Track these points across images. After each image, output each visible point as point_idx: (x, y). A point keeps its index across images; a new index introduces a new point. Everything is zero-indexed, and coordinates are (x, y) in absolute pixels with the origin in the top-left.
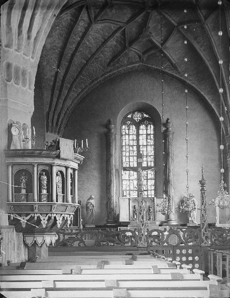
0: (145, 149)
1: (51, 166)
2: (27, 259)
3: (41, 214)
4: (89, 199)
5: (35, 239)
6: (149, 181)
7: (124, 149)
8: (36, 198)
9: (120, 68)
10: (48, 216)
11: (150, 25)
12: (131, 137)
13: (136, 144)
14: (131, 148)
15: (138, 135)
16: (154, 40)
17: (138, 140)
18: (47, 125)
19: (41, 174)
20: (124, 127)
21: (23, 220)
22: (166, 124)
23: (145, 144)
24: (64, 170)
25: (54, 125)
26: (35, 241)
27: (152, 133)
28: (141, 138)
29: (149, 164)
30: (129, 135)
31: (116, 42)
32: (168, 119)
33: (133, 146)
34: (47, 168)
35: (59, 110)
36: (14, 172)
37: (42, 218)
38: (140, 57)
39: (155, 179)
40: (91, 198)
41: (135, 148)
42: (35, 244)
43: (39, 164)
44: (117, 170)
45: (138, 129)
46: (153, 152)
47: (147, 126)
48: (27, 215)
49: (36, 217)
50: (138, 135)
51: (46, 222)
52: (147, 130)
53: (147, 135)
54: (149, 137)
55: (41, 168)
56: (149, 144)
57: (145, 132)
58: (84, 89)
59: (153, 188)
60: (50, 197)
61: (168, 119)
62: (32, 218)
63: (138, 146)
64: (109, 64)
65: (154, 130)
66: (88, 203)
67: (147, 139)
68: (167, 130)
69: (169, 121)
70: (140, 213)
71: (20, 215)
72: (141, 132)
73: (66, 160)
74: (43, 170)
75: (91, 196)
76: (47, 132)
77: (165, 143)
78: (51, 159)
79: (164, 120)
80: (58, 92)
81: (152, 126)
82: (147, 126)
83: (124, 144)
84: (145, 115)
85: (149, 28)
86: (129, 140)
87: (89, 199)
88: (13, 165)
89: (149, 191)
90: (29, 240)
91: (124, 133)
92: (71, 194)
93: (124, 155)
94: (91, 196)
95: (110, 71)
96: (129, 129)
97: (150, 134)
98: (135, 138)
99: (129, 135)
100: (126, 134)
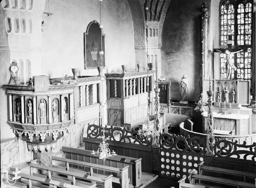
0: (242, 28)
2: (33, 158)
3: (29, 132)
4: (183, 78)
6: (246, 60)
7: (222, 29)
12: (229, 17)
13: (234, 23)
14: (229, 27)
15: (236, 14)
17: (236, 19)
20: (222, 7)
23: (243, 22)
24: (46, 98)
27: (250, 11)
28: (239, 17)
29: (247, 43)
30: (227, 14)
33: (231, 25)
34: (31, 98)
36: (14, 99)
37: (29, 135)
39: (252, 58)
41: (233, 27)
44: (209, 51)
45: (236, 8)
46: (250, 31)
47: (245, 5)
50: (236, 14)
51: (32, 138)
52: (245, 8)
53: (245, 13)
54: (246, 16)
56: (247, 23)
57: (243, 11)
59: (249, 67)
63: (236, 25)
67: (245, 18)
71: (19, 131)
72: (239, 11)
73: (152, 48)
82: (245, 5)
83: (222, 23)
86: (227, 20)
89: (246, 70)
91: (222, 13)
93: (222, 34)
96: (227, 9)
97: (248, 13)
98: (233, 17)
99: (227, 14)
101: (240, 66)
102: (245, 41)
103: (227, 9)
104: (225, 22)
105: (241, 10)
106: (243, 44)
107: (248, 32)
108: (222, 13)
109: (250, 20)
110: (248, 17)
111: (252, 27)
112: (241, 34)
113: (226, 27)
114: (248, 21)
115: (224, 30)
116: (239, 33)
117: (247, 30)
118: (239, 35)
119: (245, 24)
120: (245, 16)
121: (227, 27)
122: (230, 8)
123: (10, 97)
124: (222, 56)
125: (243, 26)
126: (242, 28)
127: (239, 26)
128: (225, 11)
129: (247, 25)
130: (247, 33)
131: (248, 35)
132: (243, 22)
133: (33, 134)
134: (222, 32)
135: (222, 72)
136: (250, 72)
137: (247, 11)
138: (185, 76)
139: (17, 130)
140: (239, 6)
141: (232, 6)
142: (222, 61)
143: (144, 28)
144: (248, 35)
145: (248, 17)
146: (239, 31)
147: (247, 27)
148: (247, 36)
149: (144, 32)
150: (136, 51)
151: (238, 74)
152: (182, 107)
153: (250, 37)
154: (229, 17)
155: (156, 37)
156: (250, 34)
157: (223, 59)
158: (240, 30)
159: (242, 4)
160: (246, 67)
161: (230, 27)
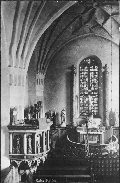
0: (93, 80)
1: (34, 134)
3: (28, 160)
4: (62, 111)
5: (25, 171)
7: (81, 80)
8: (25, 152)
9: (79, 36)
10: (32, 161)
11: (96, 14)
14: (85, 79)
16: (98, 22)
17: (89, 75)
18: (37, 70)
19: (28, 137)
20: (81, 67)
21: (18, 163)
22: (105, 67)
25: (41, 69)
26: (25, 172)
27: (97, 70)
28: (90, 74)
29: (95, 89)
31: (77, 22)
32: (106, 65)
34: (32, 134)
35: (44, 60)
36: (13, 137)
37: (28, 162)
38: (90, 30)
40: (63, 110)
41: (87, 79)
42: (25, 174)
43: (27, 133)
45: (89, 68)
46: (97, 82)
47: (94, 67)
48: (20, 161)
49: (25, 162)
50: (89, 72)
52: (94, 69)
53: (95, 72)
55: (28, 135)
57: (93, 70)
58: (58, 47)
60: (33, 152)
61: (106, 65)
62: (23, 162)
64: (72, 34)
65: (98, 68)
66: (61, 113)
67: (94, 74)
68: (106, 71)
69: (107, 66)
70: (87, 139)
71: (17, 160)
72: (91, 70)
74: (29, 136)
75: (63, 109)
76: (37, 73)
77: (104, 87)
78: (34, 130)
79: (103, 65)
80: (43, 51)
81: (97, 67)
83: (81, 77)
84: (93, 60)
85: (95, 16)
87: (62, 111)
88: (12, 133)
90: (22, 172)
92: (46, 144)
94: (63, 109)
95: (73, 38)
96: (84, 68)
97: (96, 72)
98: (87, 74)
100: (82, 71)
102: (94, 88)
103: (84, 68)
105: (92, 70)
106: (93, 89)
108: (81, 71)
109: (97, 76)
110: (96, 74)
112: (92, 84)
113: (83, 79)
114: (96, 76)
115: (82, 81)
116: (91, 83)
119: (94, 78)
120: (94, 73)
122: (85, 68)
123: (11, 135)
126: (93, 80)
128: (83, 70)
131: (96, 84)
132: (93, 77)
133: (32, 161)
135: (81, 106)
136: (97, 106)
137: (95, 71)
138: (65, 109)
139: (15, 160)
140: (91, 67)
141: (87, 67)
142: (81, 100)
144: (96, 84)
145: (96, 74)
146: (91, 82)
147: (95, 80)
150: (29, 94)
152: (60, 129)
154: (85, 73)
155: (40, 85)
158: (92, 81)
159: (92, 67)
160: (95, 103)
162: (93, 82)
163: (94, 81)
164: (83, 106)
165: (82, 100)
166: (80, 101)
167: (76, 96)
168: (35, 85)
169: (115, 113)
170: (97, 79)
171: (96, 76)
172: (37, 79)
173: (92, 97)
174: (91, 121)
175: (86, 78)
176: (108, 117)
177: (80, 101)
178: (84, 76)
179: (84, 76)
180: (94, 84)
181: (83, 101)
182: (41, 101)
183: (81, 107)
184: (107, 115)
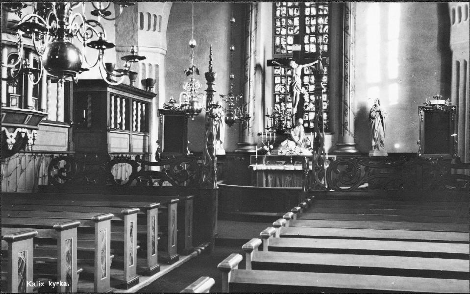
0: (313, 22)
7: (278, 24)
14: (290, 21)
41: (296, 21)
46: (327, 27)
56: (321, 13)
63: (302, 17)
101: (308, 88)
102: (317, 45)
104: (284, 12)
106: (314, 51)
107: (323, 29)
111: (328, 20)
112: (311, 33)
113: (284, 20)
114: (323, 10)
116: (308, 32)
117: (322, 26)
118: (307, 34)
121: (287, 22)
124: (279, 73)
125: (315, 20)
127: (307, 18)
129: (321, 18)
130: (321, 31)
131: (322, 34)
134: (277, 29)
135: (278, 100)
143: (137, 12)
144: (322, 34)
146: (307, 28)
148: (320, 37)
149: (136, 18)
151: (305, 104)
153: (327, 38)
156: (325, 33)
157: (279, 78)
158: (310, 26)
161: (293, 20)
162: (313, 29)
163: (317, 25)
164: (282, 100)
165: (281, 83)
166: (274, 85)
167: (258, 67)
168: (135, 31)
169: (373, 114)
170: (327, 18)
171: (323, 10)
172: (142, 15)
173: (301, 66)
174: (296, 139)
175: (294, 16)
176: (351, 127)
177: (274, 85)
178: (288, 11)
179: (288, 11)
180: (317, 34)
181: (284, 85)
182: (154, 78)
183: (279, 103)
184: (351, 119)
